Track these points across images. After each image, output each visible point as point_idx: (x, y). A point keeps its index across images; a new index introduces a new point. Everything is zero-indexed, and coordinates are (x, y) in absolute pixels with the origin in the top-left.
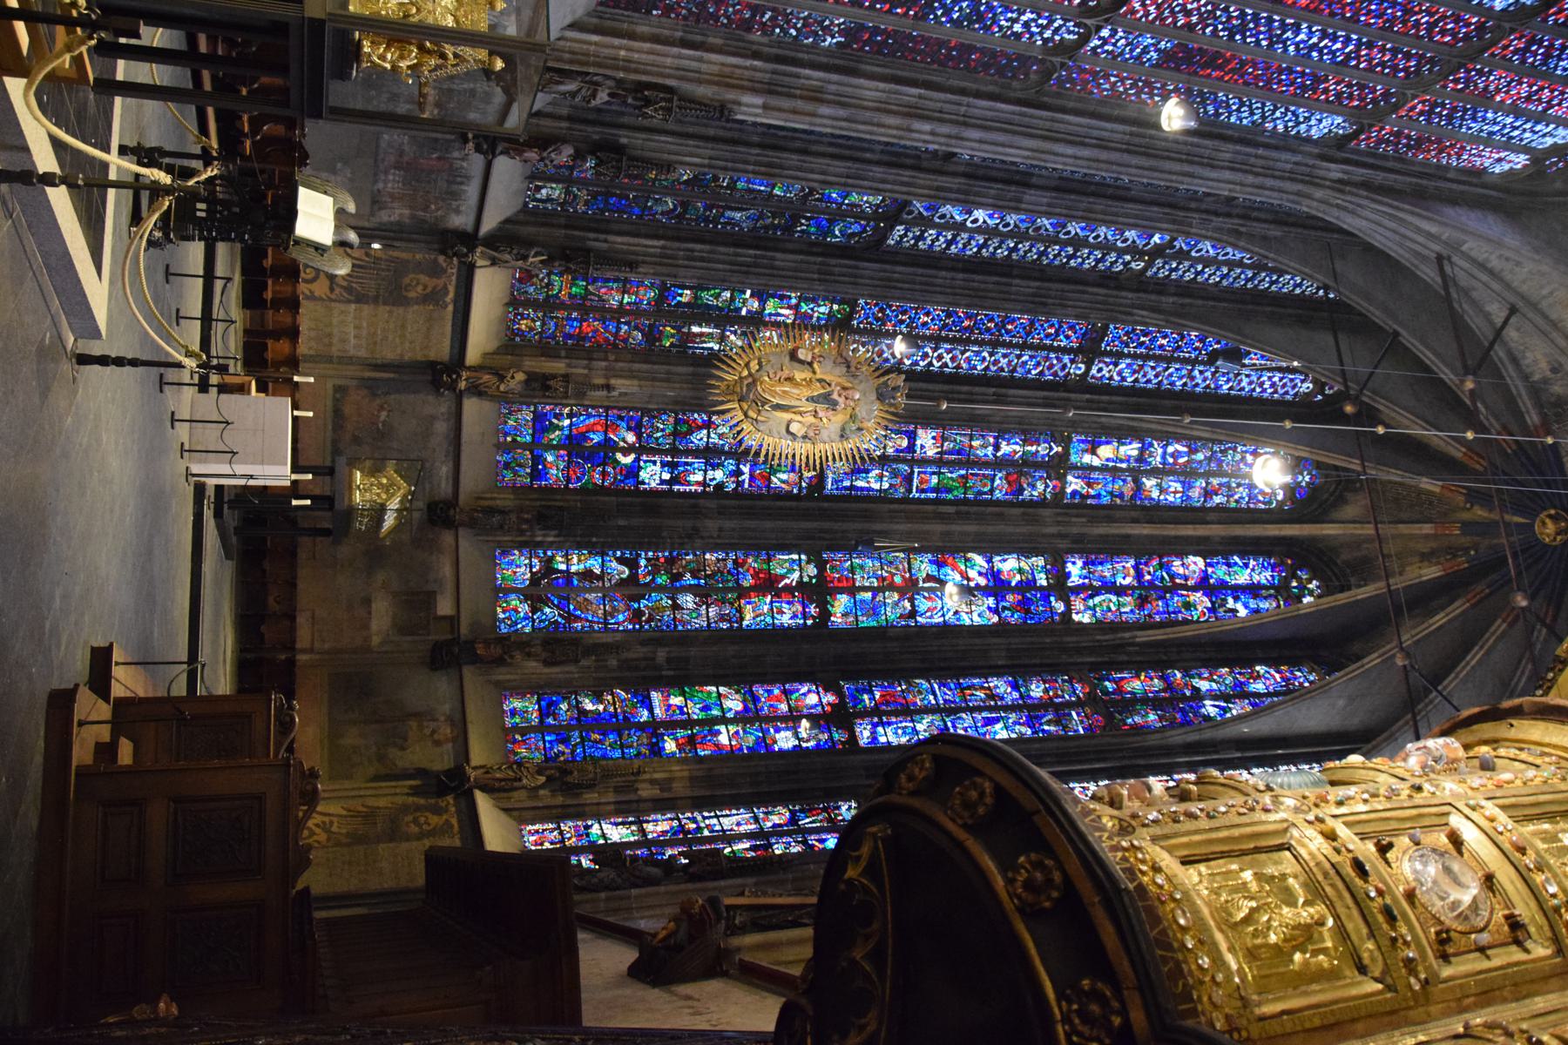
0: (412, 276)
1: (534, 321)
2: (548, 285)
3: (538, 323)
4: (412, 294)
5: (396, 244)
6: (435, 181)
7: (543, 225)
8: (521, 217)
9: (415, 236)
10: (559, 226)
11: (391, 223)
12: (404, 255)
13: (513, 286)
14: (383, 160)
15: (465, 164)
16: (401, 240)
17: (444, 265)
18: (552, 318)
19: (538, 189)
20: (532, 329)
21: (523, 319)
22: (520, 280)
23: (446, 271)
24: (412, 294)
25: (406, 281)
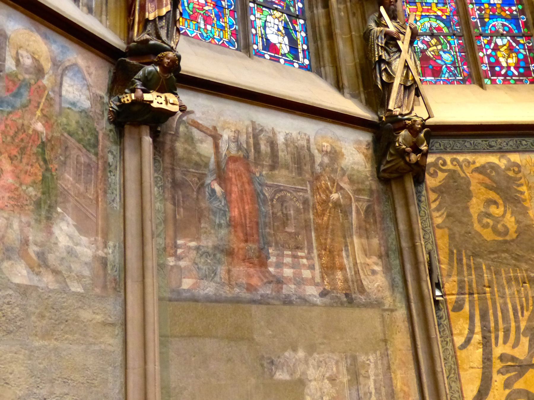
0: (477, 227)
1: (496, 48)
2: (432, 35)
3: (499, 42)
4: (510, 221)
5: (424, 257)
6: (278, 189)
7: (331, 36)
8: (329, 69)
9: (402, 227)
10: (328, 15)
11: (388, 269)
12: (443, 243)
13: (447, 82)
14: (250, 288)
15: (226, 135)
16: (414, 248)
17: (441, 176)
18: (484, 24)
19: (270, 47)
20: (511, 49)
21: (498, 63)
22: (437, 72)
23: (452, 174)
24: (510, 221)
25: (488, 235)
